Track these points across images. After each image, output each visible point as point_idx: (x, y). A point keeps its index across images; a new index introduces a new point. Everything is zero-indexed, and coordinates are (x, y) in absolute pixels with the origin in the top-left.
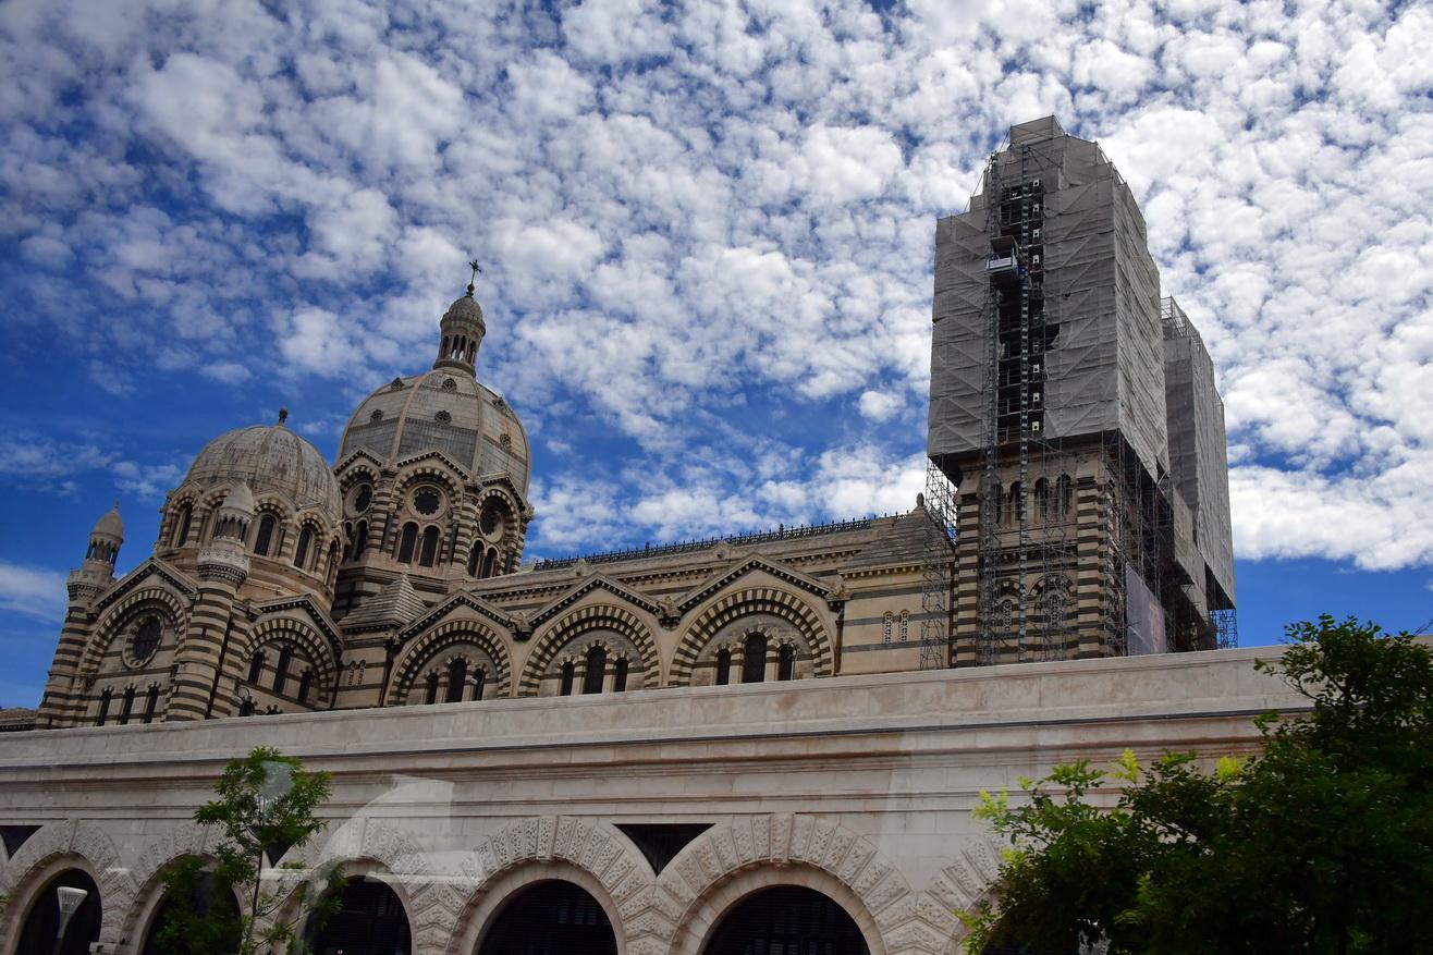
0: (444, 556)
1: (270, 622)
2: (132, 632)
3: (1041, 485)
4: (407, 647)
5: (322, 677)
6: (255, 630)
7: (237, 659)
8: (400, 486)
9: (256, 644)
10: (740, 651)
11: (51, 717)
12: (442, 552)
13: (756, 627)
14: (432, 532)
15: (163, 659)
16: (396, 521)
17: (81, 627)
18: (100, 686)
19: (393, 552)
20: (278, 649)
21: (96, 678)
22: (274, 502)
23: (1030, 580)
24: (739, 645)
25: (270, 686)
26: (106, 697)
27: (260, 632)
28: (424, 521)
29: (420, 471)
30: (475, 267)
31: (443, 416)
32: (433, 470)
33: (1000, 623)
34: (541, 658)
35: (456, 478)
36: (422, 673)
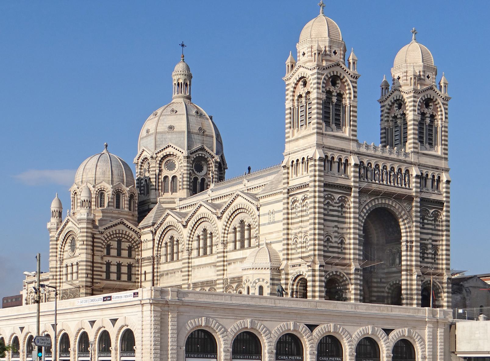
0: (180, 187)
1: (109, 233)
2: (69, 243)
4: (157, 232)
6: (104, 237)
7: (99, 249)
8: (158, 162)
9: (106, 241)
12: (180, 186)
13: (242, 218)
14: (174, 177)
15: (77, 252)
16: (160, 177)
17: (55, 242)
20: (116, 241)
21: (62, 261)
23: (300, 197)
24: (238, 225)
25: (116, 254)
26: (67, 266)
27: (106, 237)
29: (165, 154)
32: (170, 152)
35: (180, 153)
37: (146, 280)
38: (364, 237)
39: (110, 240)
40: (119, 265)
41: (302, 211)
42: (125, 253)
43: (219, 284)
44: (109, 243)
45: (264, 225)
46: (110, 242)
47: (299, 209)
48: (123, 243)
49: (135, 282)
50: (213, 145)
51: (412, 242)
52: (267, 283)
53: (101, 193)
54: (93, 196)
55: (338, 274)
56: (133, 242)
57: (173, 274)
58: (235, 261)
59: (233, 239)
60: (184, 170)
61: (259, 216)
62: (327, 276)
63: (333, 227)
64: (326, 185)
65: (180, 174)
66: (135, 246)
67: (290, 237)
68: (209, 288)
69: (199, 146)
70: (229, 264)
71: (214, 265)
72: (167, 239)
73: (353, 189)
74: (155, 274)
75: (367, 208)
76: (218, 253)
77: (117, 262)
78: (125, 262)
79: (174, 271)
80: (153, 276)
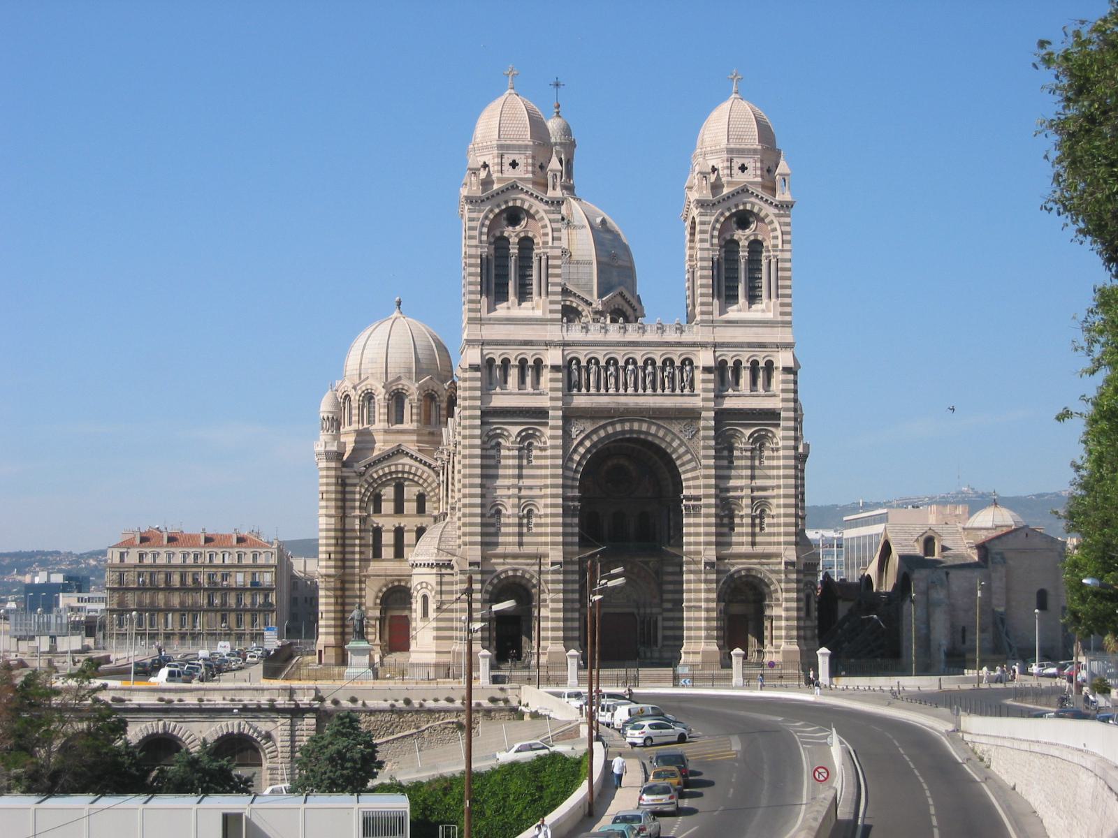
5: (432, 494)
6: (366, 481)
22: (369, 387)
30: (557, 85)
38: (580, 499)
39: (379, 485)
40: (399, 532)
42: (410, 507)
44: (377, 491)
46: (380, 488)
48: (405, 489)
50: (591, 280)
51: (698, 498)
53: (369, 397)
54: (355, 405)
55: (519, 574)
56: (425, 485)
62: (493, 579)
63: (509, 489)
66: (431, 491)
73: (551, 413)
75: (588, 444)
77: (394, 526)
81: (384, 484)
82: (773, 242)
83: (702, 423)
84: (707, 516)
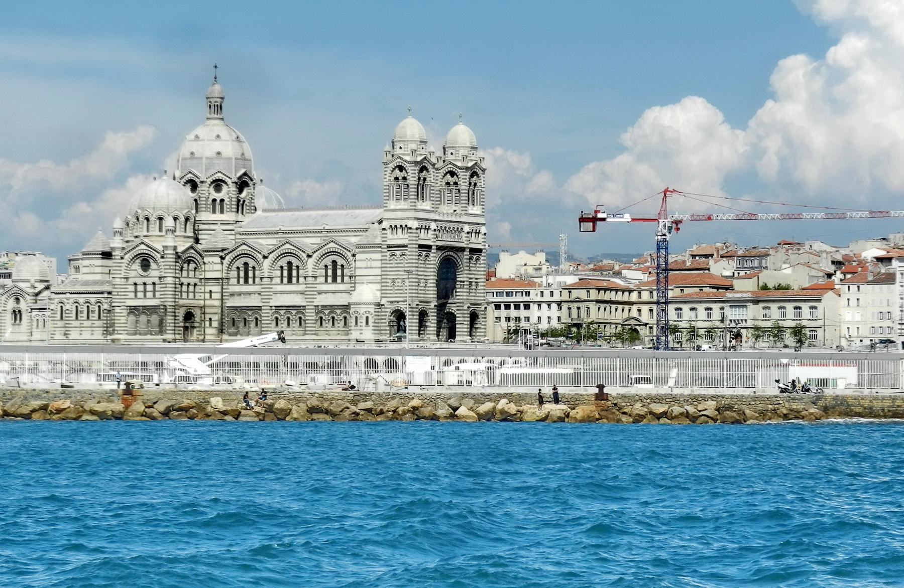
3: (401, 226)
4: (228, 258)
8: (208, 186)
10: (330, 265)
11: (118, 292)
14: (222, 201)
18: (131, 281)
19: (209, 211)
23: (398, 253)
28: (218, 196)
30: (216, 67)
31: (219, 153)
33: (392, 264)
34: (273, 264)
35: (229, 180)
36: (234, 266)
37: (213, 297)
41: (399, 263)
43: (308, 309)
45: (361, 268)
47: (396, 262)
49: (199, 300)
51: (464, 282)
52: (372, 314)
57: (248, 296)
58: (326, 292)
59: (324, 274)
60: (233, 194)
61: (355, 261)
64: (420, 246)
65: (229, 198)
67: (388, 281)
68: (295, 311)
69: (243, 171)
70: (319, 293)
71: (302, 293)
72: (240, 263)
73: (433, 247)
74: (224, 294)
76: (306, 284)
78: (192, 281)
79: (249, 294)
80: (222, 296)
81: (185, 263)
82: (480, 184)
83: (465, 253)
84: (467, 289)
